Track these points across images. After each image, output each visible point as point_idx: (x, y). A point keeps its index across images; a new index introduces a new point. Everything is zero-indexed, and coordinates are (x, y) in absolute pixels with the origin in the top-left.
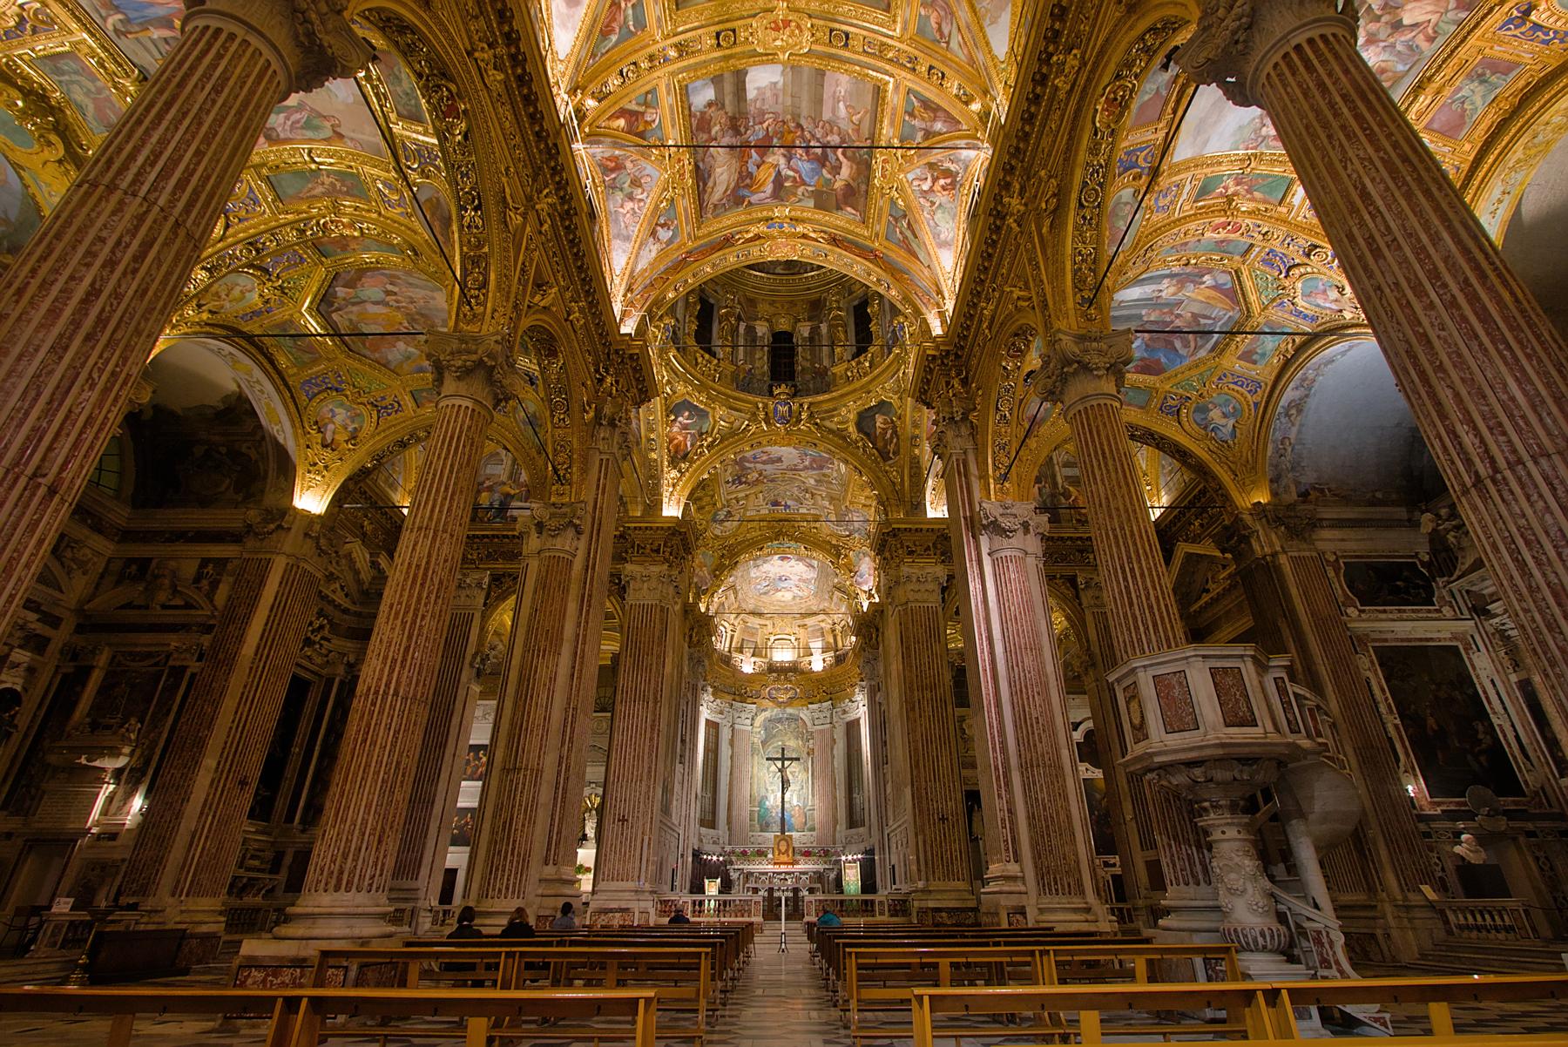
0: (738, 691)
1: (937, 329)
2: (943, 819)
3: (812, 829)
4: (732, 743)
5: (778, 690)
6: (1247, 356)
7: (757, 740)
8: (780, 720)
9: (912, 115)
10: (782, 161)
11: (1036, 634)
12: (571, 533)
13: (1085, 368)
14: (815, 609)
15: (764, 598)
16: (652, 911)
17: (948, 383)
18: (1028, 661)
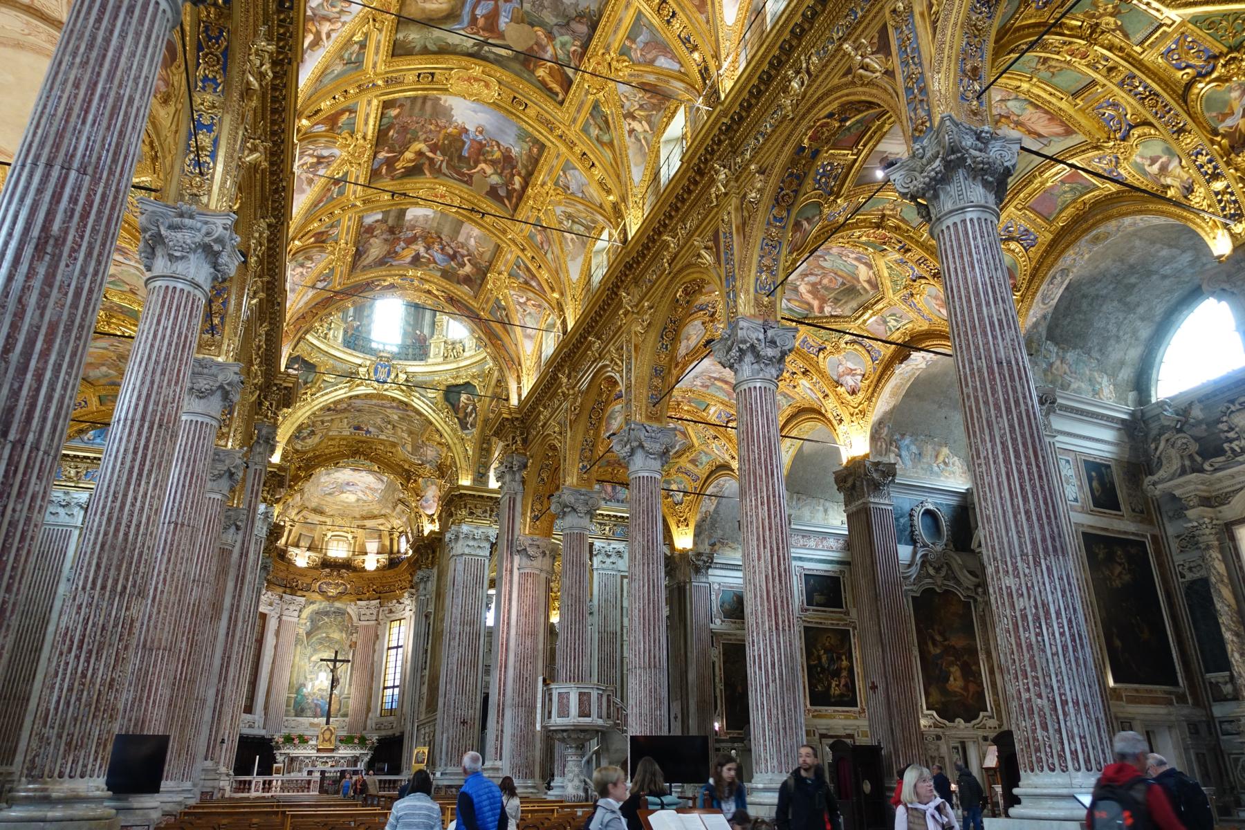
0: (289, 582)
1: (514, 401)
2: (464, 723)
3: (345, 715)
4: (277, 634)
5: (328, 584)
6: (693, 462)
7: (302, 631)
8: (327, 613)
9: (518, 267)
10: (422, 251)
11: (536, 624)
12: (233, 527)
13: (574, 510)
14: (376, 512)
15: (329, 498)
16: (228, 789)
17: (514, 438)
18: (528, 642)
